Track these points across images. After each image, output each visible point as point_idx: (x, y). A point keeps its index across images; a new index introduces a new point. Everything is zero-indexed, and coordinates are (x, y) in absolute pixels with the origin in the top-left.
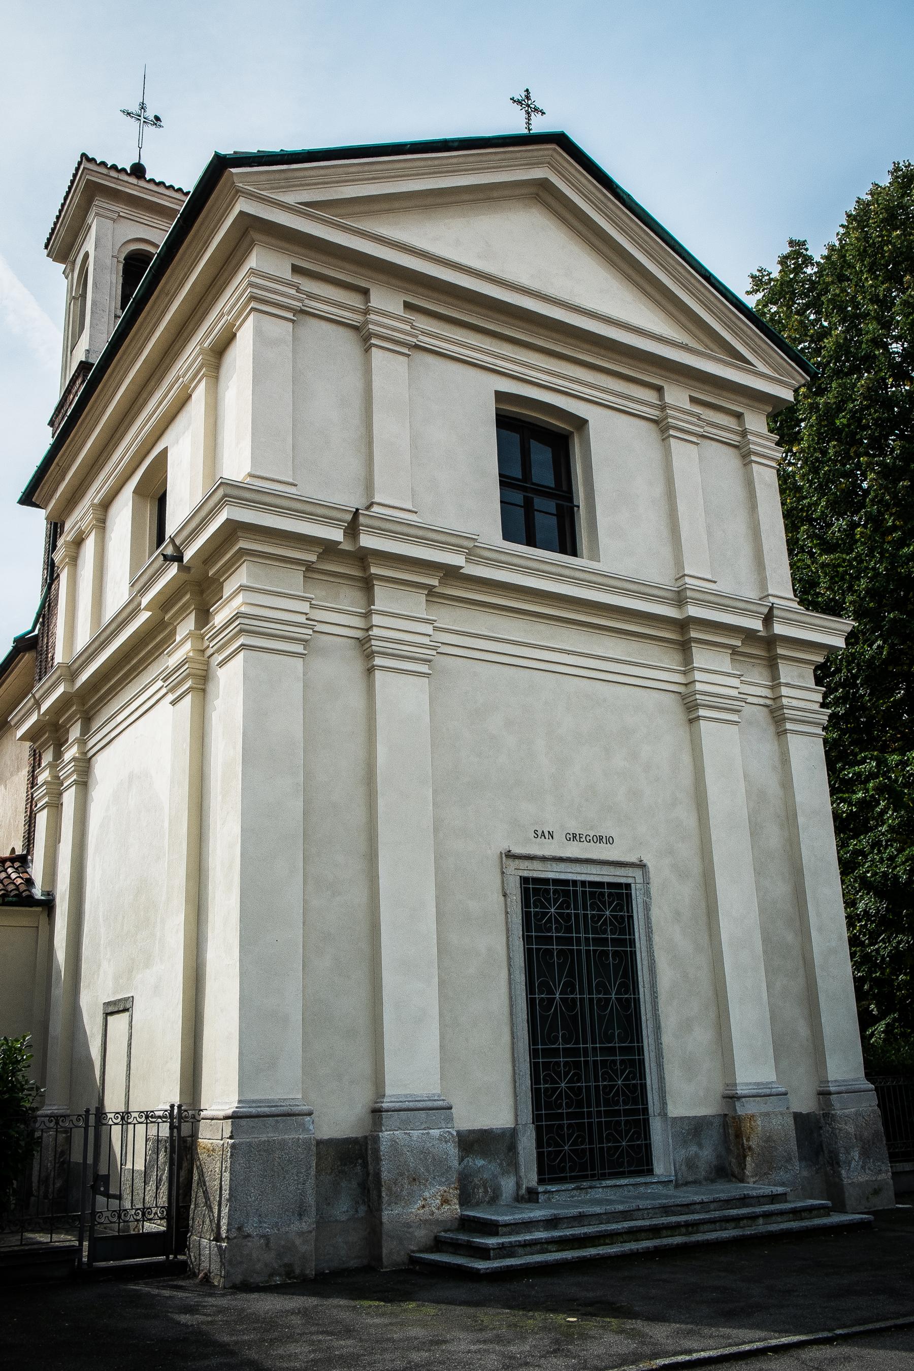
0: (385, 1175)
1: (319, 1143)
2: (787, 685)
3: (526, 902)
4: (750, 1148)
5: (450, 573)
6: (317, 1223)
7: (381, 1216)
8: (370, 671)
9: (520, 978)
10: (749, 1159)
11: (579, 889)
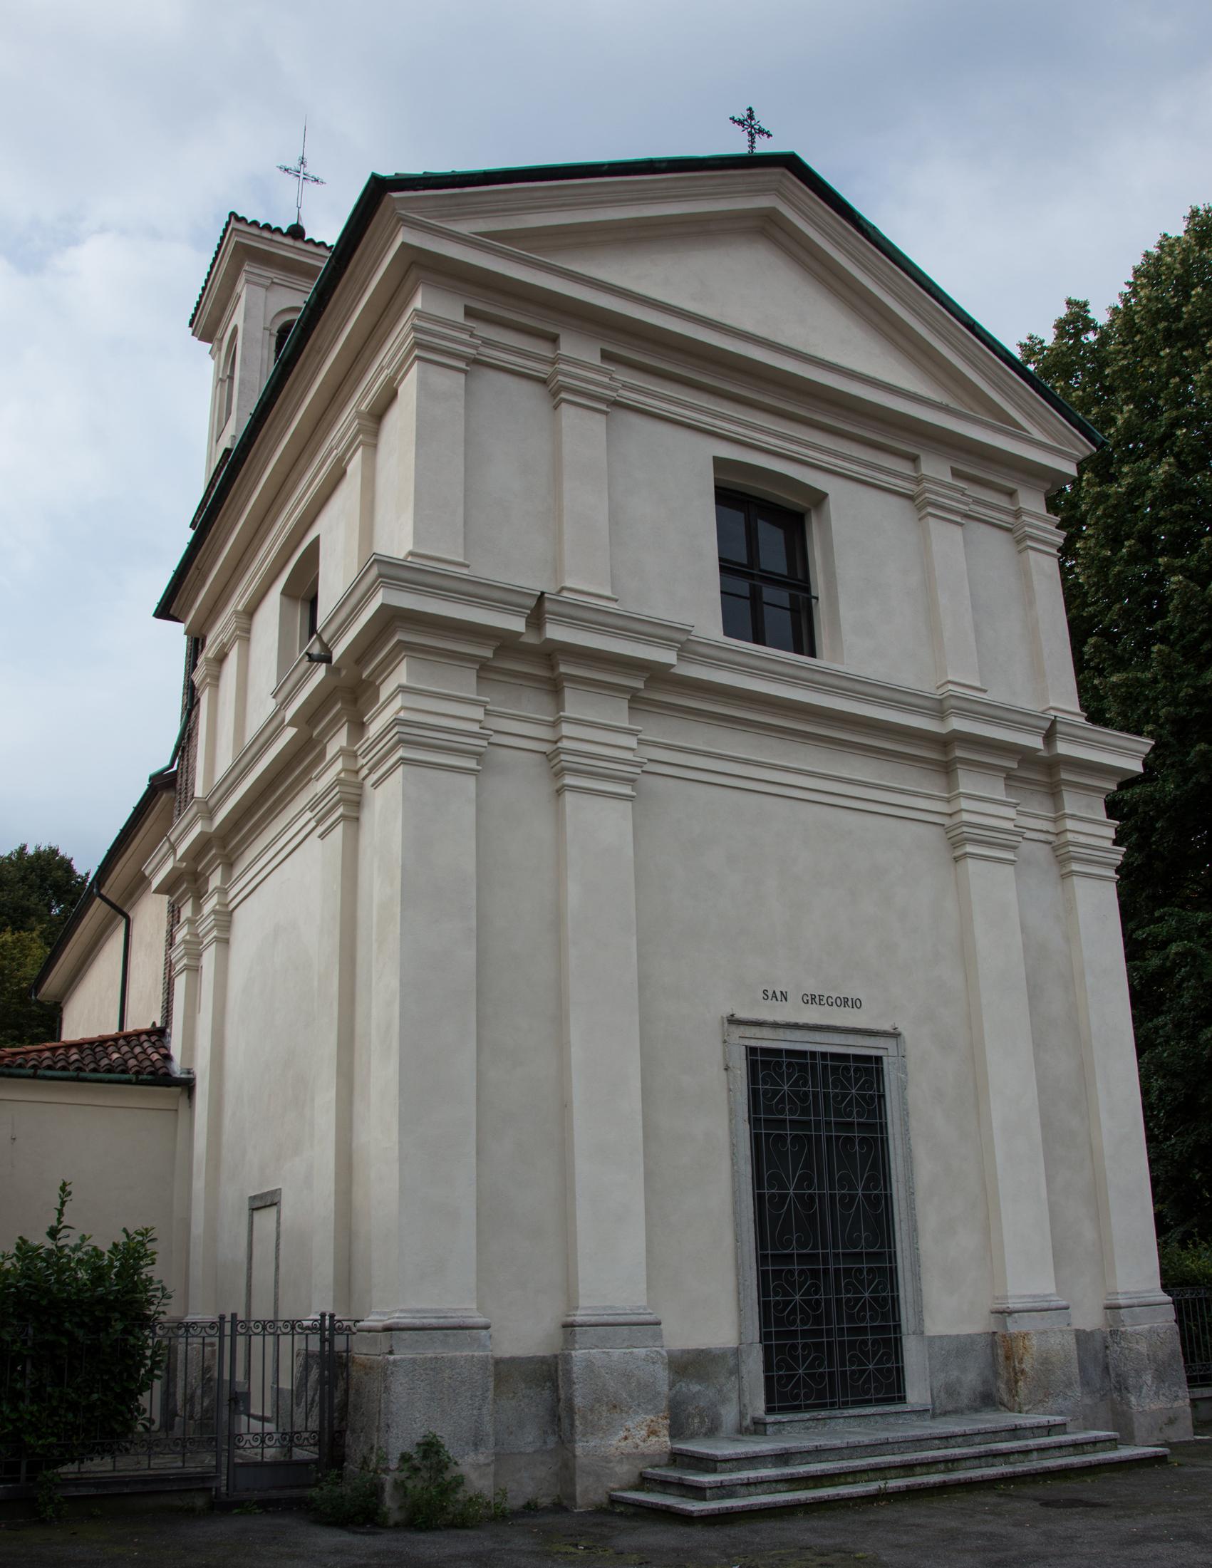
0: (578, 1401)
1: (498, 1362)
2: (1073, 817)
4: (1023, 1371)
5: (657, 674)
6: (496, 1454)
7: (574, 1448)
9: (747, 1169)
10: (1021, 1383)
11: (818, 1061)
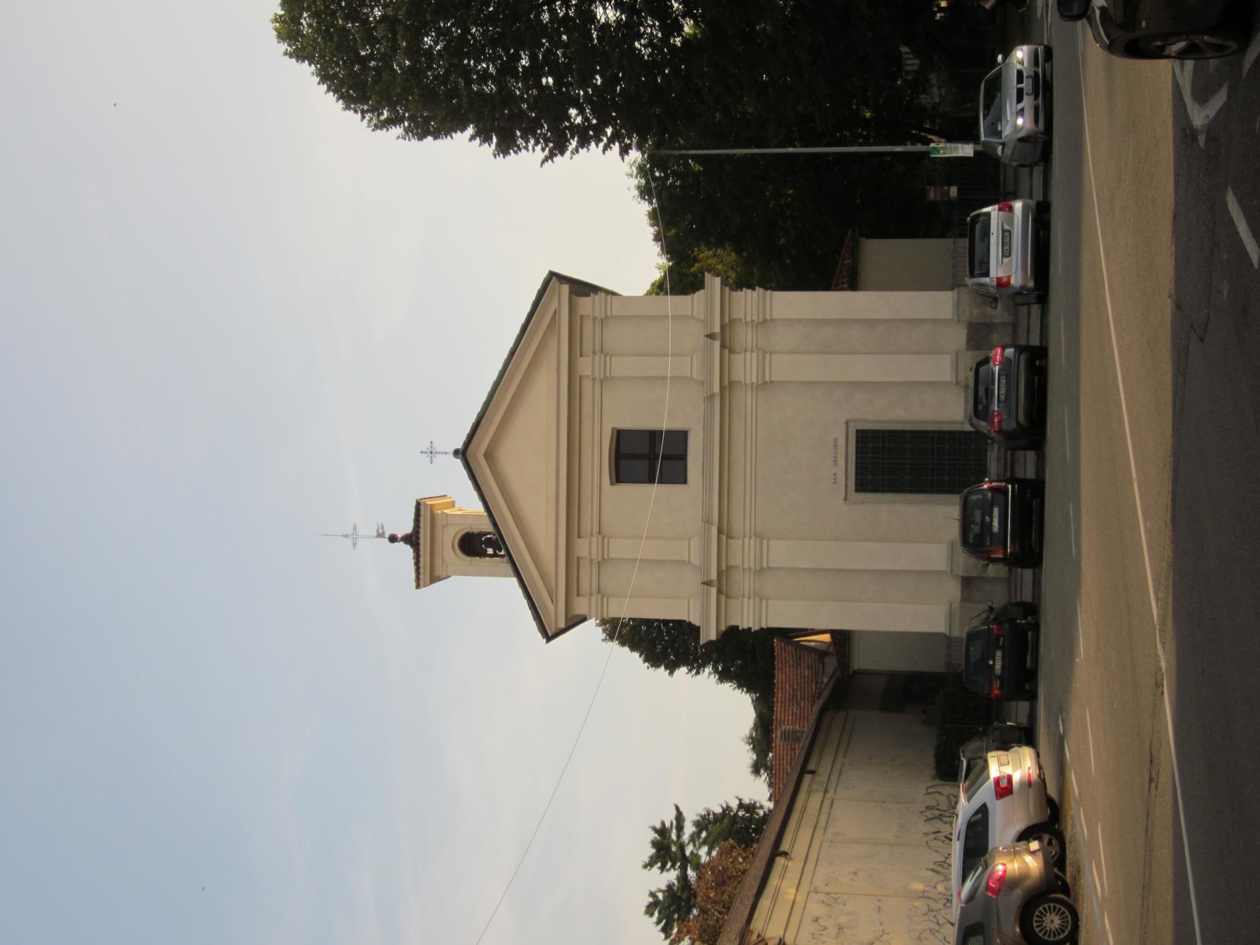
3: (860, 451)
5: (720, 531)
8: (769, 568)
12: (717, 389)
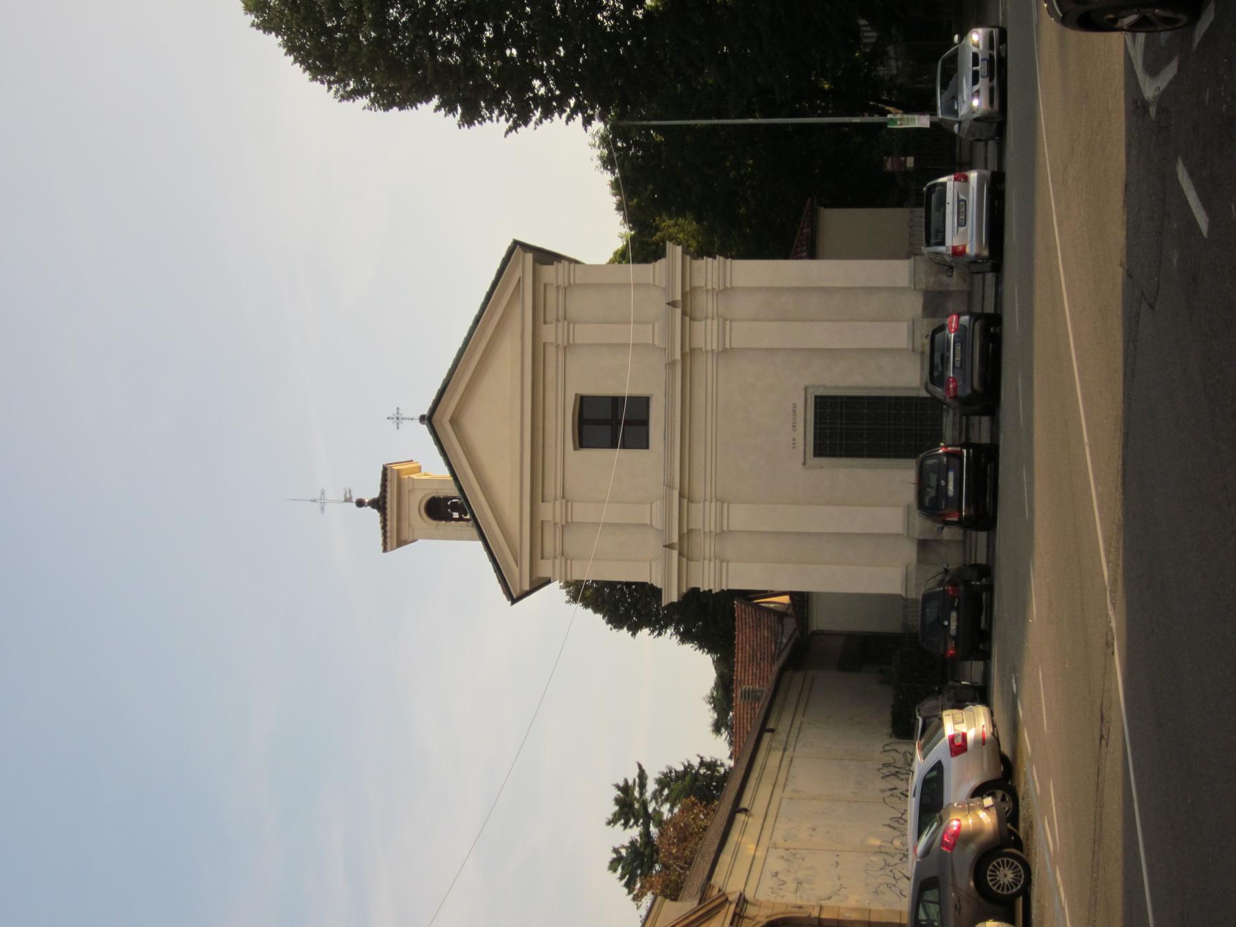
5: (681, 495)
8: (730, 532)
12: (678, 356)
